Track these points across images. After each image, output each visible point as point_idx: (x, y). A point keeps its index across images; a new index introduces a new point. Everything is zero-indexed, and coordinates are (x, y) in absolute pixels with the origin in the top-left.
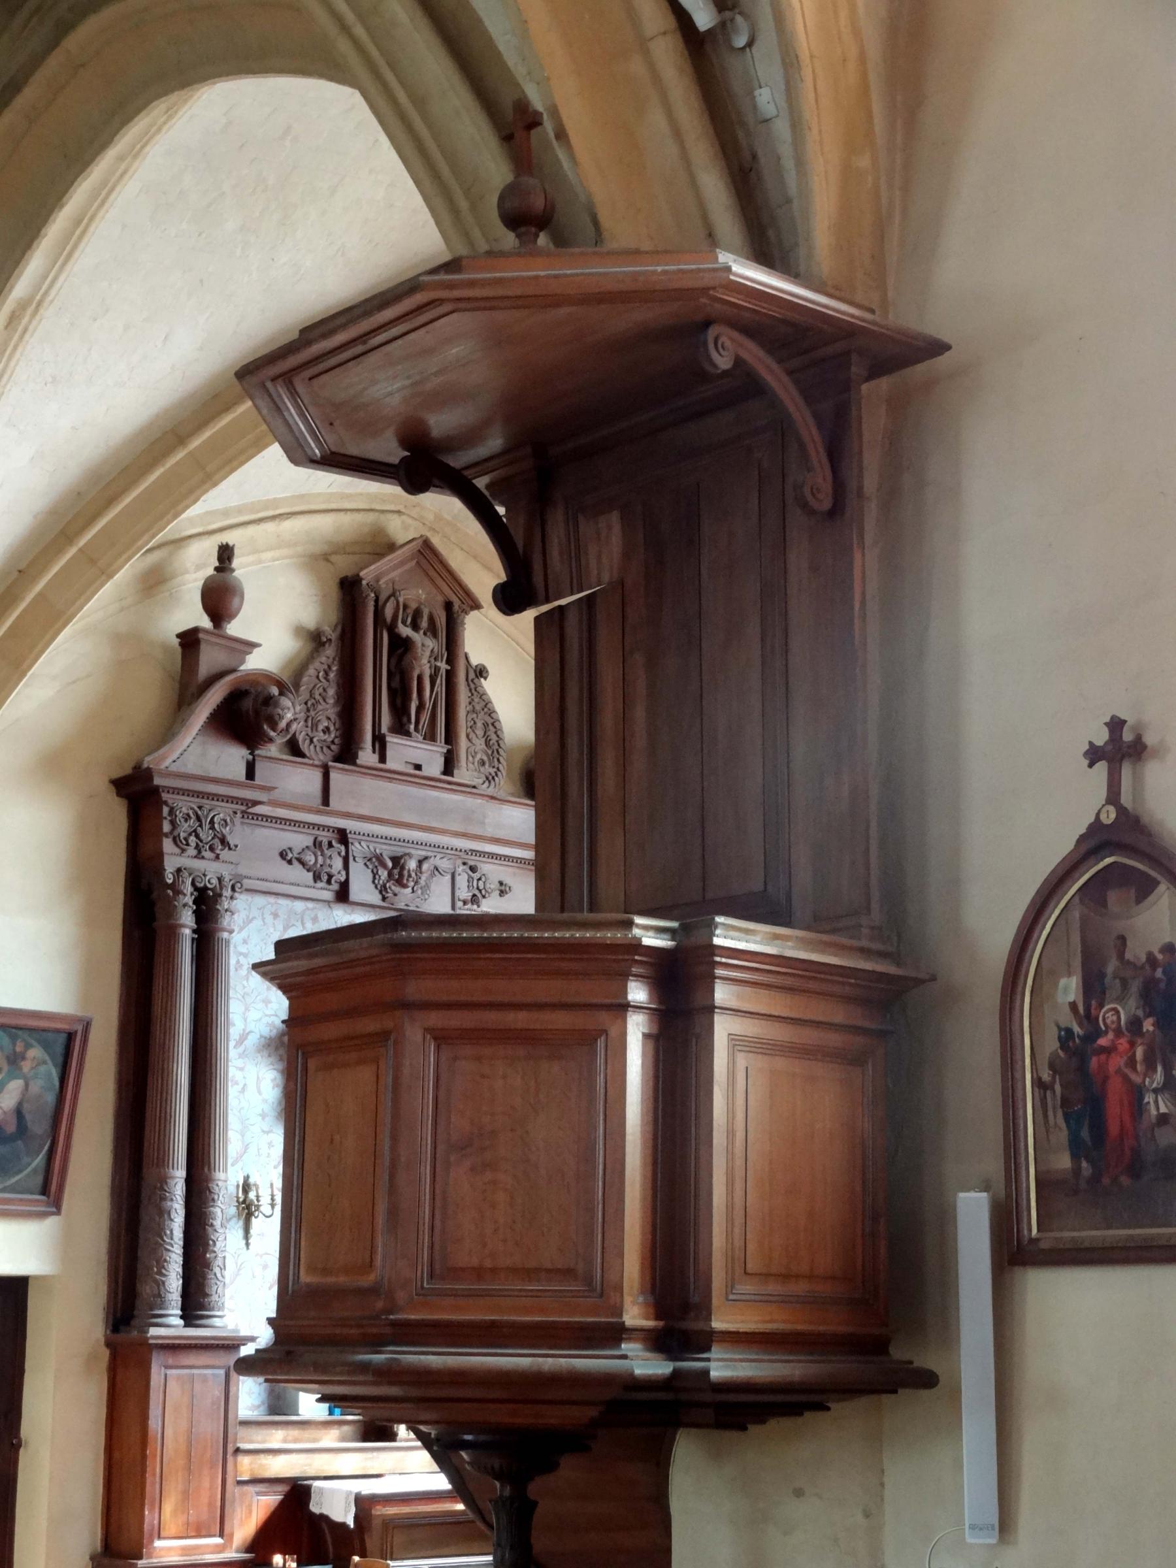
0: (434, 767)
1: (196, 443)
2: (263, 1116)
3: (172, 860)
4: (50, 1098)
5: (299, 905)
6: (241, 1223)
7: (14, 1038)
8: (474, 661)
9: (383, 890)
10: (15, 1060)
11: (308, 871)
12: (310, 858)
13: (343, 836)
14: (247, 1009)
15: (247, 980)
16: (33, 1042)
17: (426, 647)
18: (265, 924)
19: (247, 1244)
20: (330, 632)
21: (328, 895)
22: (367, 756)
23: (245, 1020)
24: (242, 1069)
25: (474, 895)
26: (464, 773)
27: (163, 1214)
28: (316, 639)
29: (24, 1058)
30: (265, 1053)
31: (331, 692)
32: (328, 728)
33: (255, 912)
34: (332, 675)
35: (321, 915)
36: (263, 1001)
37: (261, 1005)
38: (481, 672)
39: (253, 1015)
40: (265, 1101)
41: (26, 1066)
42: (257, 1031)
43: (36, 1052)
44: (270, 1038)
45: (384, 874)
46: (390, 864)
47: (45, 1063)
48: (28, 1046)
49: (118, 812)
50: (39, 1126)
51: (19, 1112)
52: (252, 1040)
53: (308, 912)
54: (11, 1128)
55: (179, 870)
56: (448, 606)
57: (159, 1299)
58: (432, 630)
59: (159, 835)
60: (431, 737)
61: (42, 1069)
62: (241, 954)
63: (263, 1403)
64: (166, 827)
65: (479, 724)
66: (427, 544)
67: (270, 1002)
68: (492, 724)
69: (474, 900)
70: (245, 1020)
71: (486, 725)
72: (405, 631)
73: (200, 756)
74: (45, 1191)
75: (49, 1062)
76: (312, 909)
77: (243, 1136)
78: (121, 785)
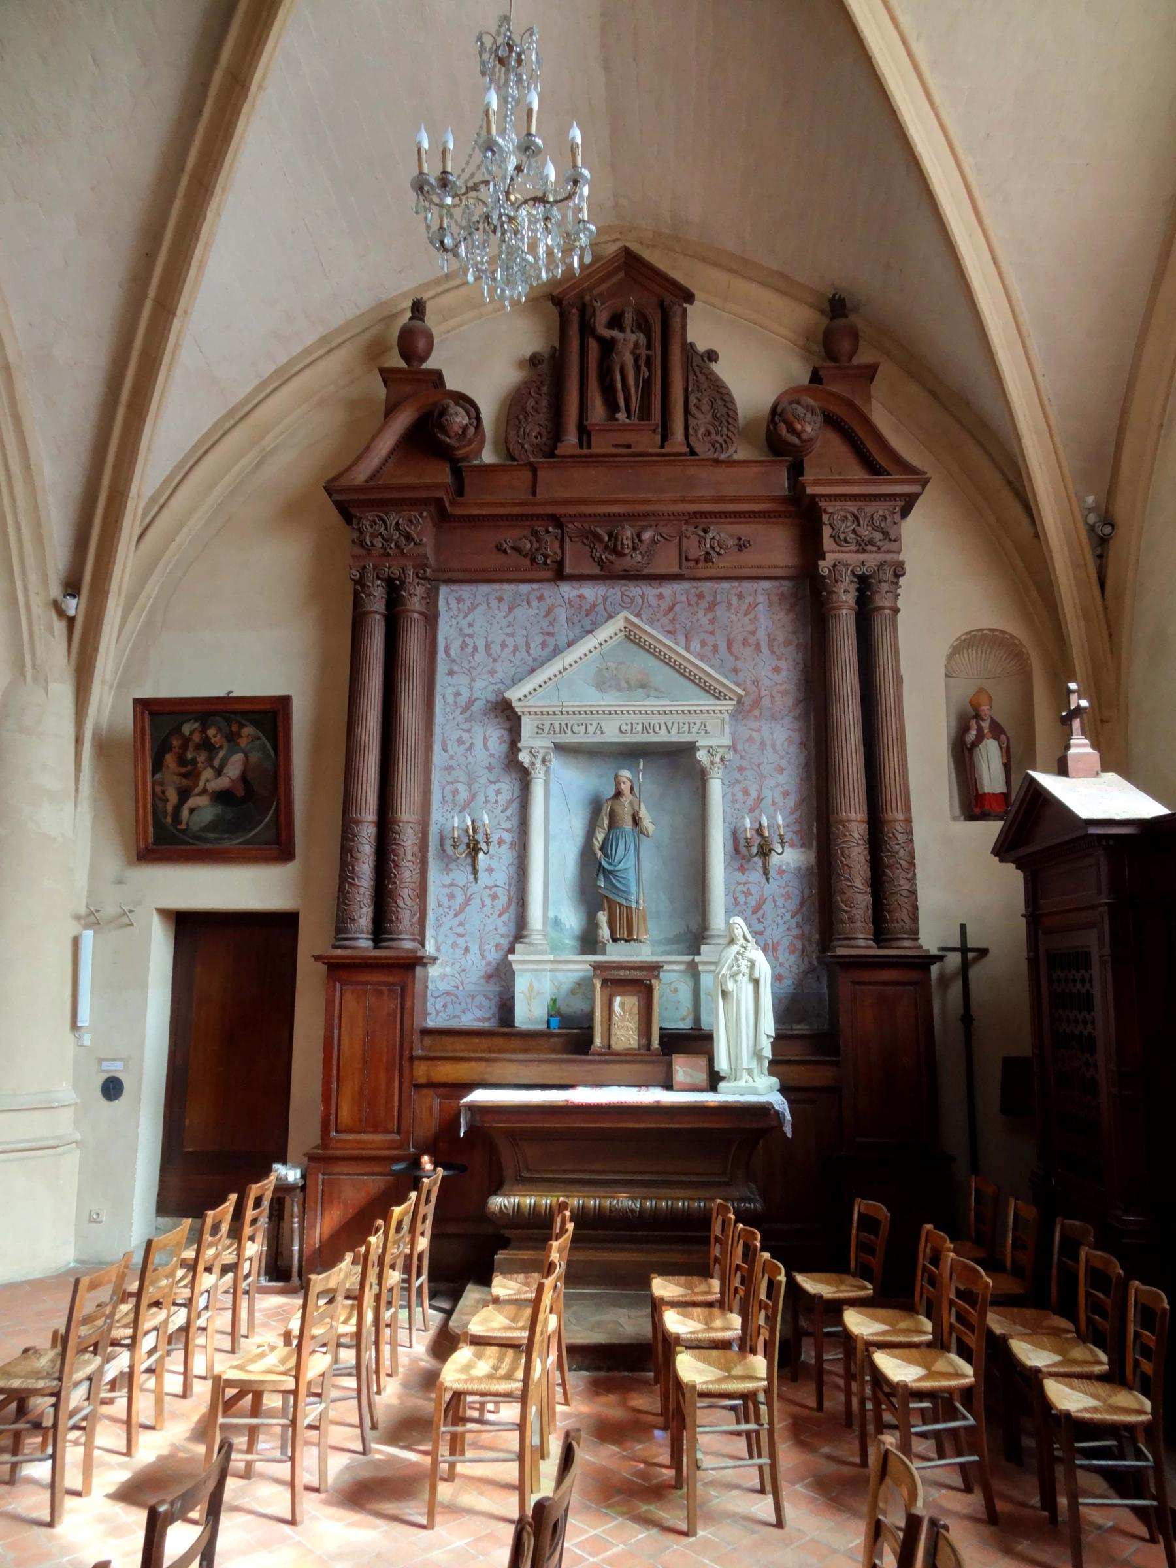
2: (490, 769)
6: (469, 860)
7: (229, 722)
8: (702, 348)
9: (600, 563)
10: (232, 739)
11: (525, 556)
14: (473, 680)
15: (473, 655)
16: (244, 722)
19: (476, 879)
21: (548, 574)
23: (471, 690)
24: (468, 731)
25: (707, 553)
29: (240, 736)
30: (492, 715)
31: (545, 403)
32: (540, 433)
33: (479, 599)
34: (545, 389)
35: (547, 594)
37: (487, 676)
38: (712, 356)
39: (479, 684)
40: (492, 756)
41: (243, 742)
42: (482, 697)
43: (249, 730)
44: (497, 703)
46: (606, 539)
47: (259, 738)
48: (242, 726)
51: (244, 778)
52: (478, 706)
54: (240, 792)
61: (257, 743)
63: (494, 1015)
65: (705, 401)
66: (628, 253)
70: (471, 690)
71: (712, 403)
74: (278, 842)
75: (264, 739)
76: (538, 590)
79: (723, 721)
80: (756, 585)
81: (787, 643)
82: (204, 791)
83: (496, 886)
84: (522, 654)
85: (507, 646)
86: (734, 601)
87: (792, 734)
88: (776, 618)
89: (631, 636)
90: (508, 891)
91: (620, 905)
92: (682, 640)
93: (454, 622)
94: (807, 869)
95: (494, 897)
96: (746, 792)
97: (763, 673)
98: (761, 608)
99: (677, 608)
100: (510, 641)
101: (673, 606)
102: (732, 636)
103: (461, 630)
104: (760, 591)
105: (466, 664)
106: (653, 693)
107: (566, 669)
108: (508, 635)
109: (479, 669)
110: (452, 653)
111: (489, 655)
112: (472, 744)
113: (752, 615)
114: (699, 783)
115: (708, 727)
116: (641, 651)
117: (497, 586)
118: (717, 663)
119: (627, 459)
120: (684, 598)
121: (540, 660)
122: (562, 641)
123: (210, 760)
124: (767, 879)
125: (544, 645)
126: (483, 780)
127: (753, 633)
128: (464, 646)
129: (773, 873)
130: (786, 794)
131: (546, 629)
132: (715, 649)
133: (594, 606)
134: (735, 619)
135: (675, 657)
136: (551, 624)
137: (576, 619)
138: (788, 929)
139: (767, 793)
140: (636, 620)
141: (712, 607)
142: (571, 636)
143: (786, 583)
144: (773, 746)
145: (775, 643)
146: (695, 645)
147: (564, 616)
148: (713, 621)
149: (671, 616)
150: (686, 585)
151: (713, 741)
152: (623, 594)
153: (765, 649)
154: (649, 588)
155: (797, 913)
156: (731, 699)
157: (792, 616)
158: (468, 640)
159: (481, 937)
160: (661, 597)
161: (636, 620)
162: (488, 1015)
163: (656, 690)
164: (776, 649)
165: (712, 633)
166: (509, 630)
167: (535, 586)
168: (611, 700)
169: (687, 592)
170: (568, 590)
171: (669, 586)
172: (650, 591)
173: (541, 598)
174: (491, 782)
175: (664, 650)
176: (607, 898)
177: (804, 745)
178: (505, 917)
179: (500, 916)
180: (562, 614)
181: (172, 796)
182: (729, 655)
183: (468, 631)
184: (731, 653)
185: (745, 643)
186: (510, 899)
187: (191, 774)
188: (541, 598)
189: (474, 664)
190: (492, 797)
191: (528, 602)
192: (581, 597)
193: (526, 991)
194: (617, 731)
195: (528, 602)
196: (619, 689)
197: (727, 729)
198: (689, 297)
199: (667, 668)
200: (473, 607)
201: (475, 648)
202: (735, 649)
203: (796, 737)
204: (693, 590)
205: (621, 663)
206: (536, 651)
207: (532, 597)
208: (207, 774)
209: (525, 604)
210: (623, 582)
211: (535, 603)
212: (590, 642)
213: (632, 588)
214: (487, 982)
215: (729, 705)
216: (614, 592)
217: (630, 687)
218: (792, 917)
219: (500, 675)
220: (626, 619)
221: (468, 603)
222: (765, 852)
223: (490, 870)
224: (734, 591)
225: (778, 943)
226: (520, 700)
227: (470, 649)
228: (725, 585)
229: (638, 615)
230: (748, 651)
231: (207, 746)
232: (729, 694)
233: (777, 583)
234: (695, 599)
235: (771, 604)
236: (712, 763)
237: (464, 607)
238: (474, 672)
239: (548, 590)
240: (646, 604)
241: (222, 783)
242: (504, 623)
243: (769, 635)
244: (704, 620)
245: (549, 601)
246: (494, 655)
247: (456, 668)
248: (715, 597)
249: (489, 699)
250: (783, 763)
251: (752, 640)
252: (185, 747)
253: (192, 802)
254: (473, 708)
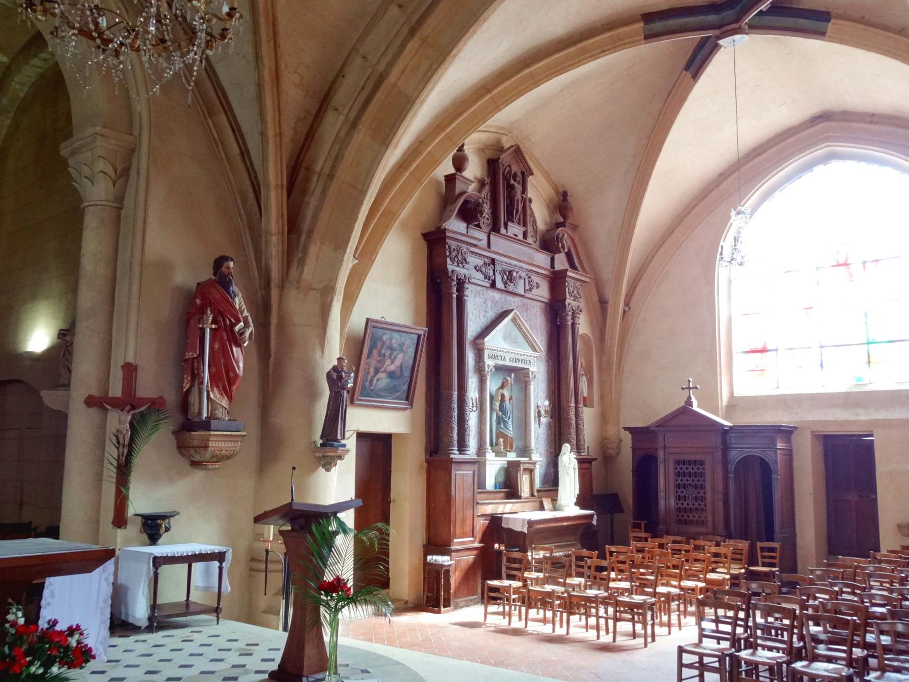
0: (520, 237)
1: (495, 92)
3: (450, 267)
4: (411, 361)
5: (479, 288)
9: (505, 283)
12: (483, 269)
13: (493, 261)
17: (519, 188)
20: (487, 180)
21: (488, 285)
22: (503, 231)
26: (530, 240)
27: (450, 409)
28: (482, 184)
45: (505, 277)
49: (424, 245)
50: (407, 374)
51: (401, 367)
54: (398, 373)
55: (453, 271)
56: (523, 173)
57: (450, 444)
58: (518, 183)
59: (446, 257)
60: (519, 224)
64: (448, 253)
68: (534, 221)
69: (530, 290)
72: (512, 182)
73: (455, 225)
78: (426, 236)
82: (385, 371)
119: (514, 239)
123: (391, 355)
150: (521, 299)
177: (548, 373)
181: (372, 371)
187: (381, 362)
198: (532, 174)
208: (388, 362)
215: (537, 354)
231: (391, 349)
241: (392, 368)
252: (382, 347)
253: (378, 376)
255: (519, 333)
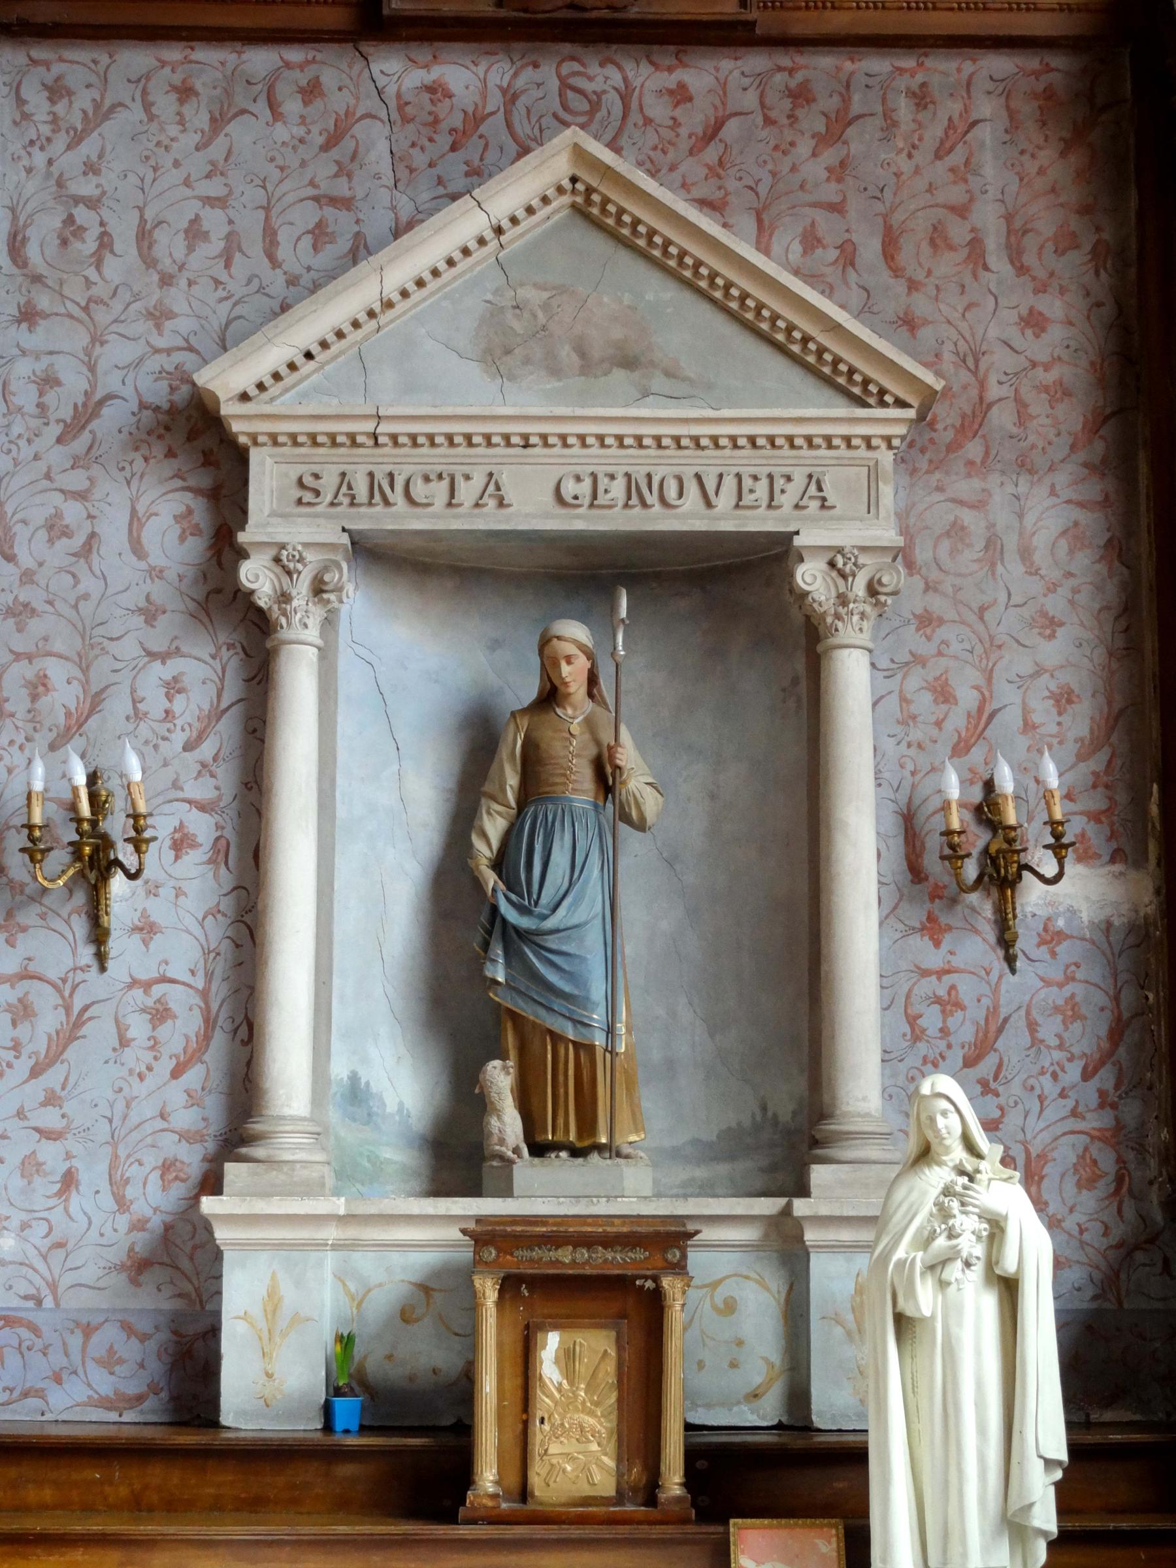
2: (150, 613)
6: (80, 898)
14: (97, 339)
15: (98, 266)
18: (151, 118)
19: (101, 959)
23: (92, 369)
24: (81, 496)
30: (158, 450)
33: (120, 90)
35: (329, 78)
36: (150, 315)
37: (142, 327)
39: (118, 352)
40: (156, 573)
42: (128, 392)
44: (173, 411)
52: (114, 419)
53: (286, 73)
62: (77, 200)
63: (154, 1389)
67: (170, 315)
70: (92, 369)
76: (302, 67)
77: (85, 670)
79: (873, 474)
80: (968, 67)
81: (1065, 243)
83: (164, 979)
84: (252, 260)
85: (205, 236)
86: (904, 109)
87: (1085, 518)
88: (1032, 167)
89: (592, 208)
90: (204, 994)
91: (557, 1038)
92: (748, 224)
93: (39, 159)
94: (1132, 928)
95: (160, 1014)
96: (943, 693)
97: (993, 333)
98: (985, 134)
99: (732, 129)
100: (214, 221)
101: (719, 125)
102: (898, 218)
103: (60, 184)
104: (982, 84)
105: (75, 291)
106: (658, 382)
107: (389, 305)
108: (208, 201)
109: (117, 306)
110: (33, 252)
111: (149, 262)
112: (93, 535)
113: (957, 157)
114: (800, 665)
115: (828, 491)
116: (624, 257)
117: (173, 53)
118: (856, 297)
120: (750, 100)
121: (306, 280)
122: (378, 221)
124: (1010, 960)
125: (320, 234)
126: (129, 649)
127: (961, 211)
128: (71, 230)
129: (1025, 942)
130: (1064, 699)
131: (325, 188)
132: (848, 256)
133: (476, 119)
134: (906, 166)
135: (728, 272)
136: (343, 171)
137: (420, 159)
138: (1074, 1113)
139: (1007, 695)
140: (607, 156)
141: (838, 127)
142: (406, 210)
143: (1058, 61)
144: (1025, 554)
145: (1031, 243)
146: (787, 240)
147: (383, 147)
148: (838, 172)
149: (711, 154)
150: (757, 61)
151: (845, 528)
152: (565, 85)
153: (998, 262)
154: (645, 69)
155: (1102, 1063)
156: (901, 403)
157: (1075, 159)
158: (82, 215)
159: (113, 1141)
160: (681, 95)
161: (607, 156)
162: (132, 1388)
163: (668, 374)
164: (1030, 259)
165: (837, 208)
166: (214, 188)
167: (295, 54)
168: (528, 402)
169: (762, 81)
170: (396, 70)
171: (708, 64)
172: (646, 77)
173: (311, 91)
174: (152, 655)
175: (696, 250)
176: (514, 1016)
177: (1118, 550)
178: (194, 1076)
179: (176, 1074)
180: (376, 143)
182: (885, 275)
183: (86, 187)
184: (897, 272)
185: (938, 239)
186: (209, 1022)
188: (311, 91)
189: (98, 291)
190: (155, 702)
191: (273, 105)
192: (435, 90)
193: (257, 1312)
194: (549, 498)
195: (273, 105)
196: (555, 371)
197: (887, 492)
199: (705, 308)
200: (101, 114)
201: (105, 242)
202: (905, 256)
203: (1092, 522)
204: (779, 78)
205: (561, 290)
206: (295, 253)
207: (283, 90)
209: (261, 107)
210: (567, 48)
211: (292, 106)
212: (463, 224)
213: (594, 69)
214: (135, 1282)
215: (892, 422)
216: (540, 76)
217: (587, 365)
218: (1086, 1075)
219: (184, 324)
220: (579, 153)
221: (84, 100)
222: (1002, 874)
223: (147, 929)
224: (902, 83)
225: (1043, 1157)
226: (244, 397)
227: (89, 245)
228: (877, 64)
229: (614, 146)
230: (947, 265)
232: (896, 389)
233: (1032, 62)
234: (787, 104)
235: (1014, 123)
236: (843, 599)
237: (73, 112)
238: (102, 316)
239: (334, 68)
240: (635, 117)
242: (197, 164)
243: (1009, 218)
244: (815, 170)
245: (338, 101)
246: (166, 264)
247: (44, 302)
248: (846, 100)
249: (150, 399)
250: (1056, 605)
251: (958, 232)
254: (94, 425)
255: (658, 291)
